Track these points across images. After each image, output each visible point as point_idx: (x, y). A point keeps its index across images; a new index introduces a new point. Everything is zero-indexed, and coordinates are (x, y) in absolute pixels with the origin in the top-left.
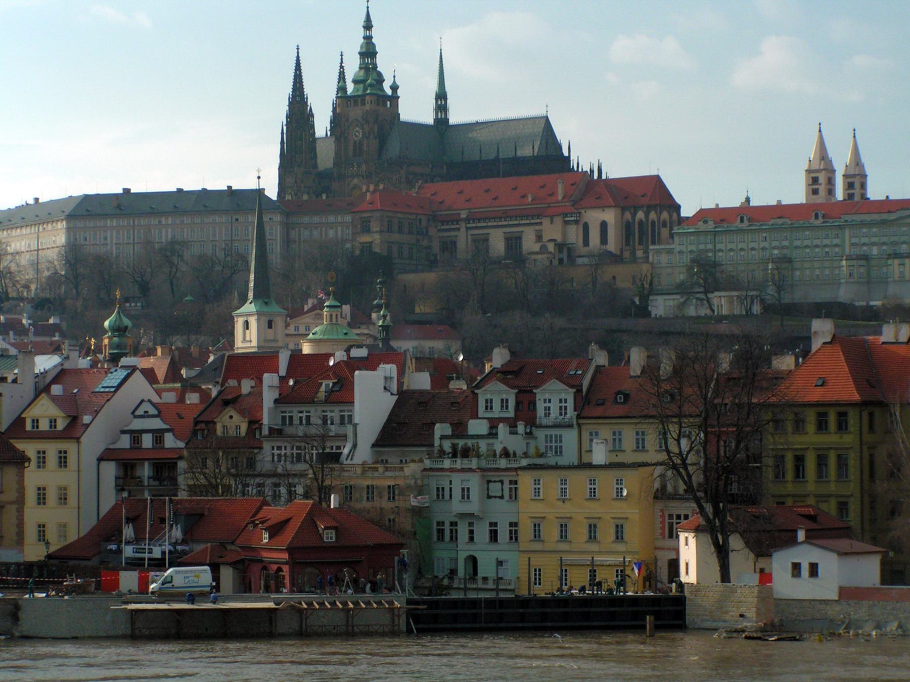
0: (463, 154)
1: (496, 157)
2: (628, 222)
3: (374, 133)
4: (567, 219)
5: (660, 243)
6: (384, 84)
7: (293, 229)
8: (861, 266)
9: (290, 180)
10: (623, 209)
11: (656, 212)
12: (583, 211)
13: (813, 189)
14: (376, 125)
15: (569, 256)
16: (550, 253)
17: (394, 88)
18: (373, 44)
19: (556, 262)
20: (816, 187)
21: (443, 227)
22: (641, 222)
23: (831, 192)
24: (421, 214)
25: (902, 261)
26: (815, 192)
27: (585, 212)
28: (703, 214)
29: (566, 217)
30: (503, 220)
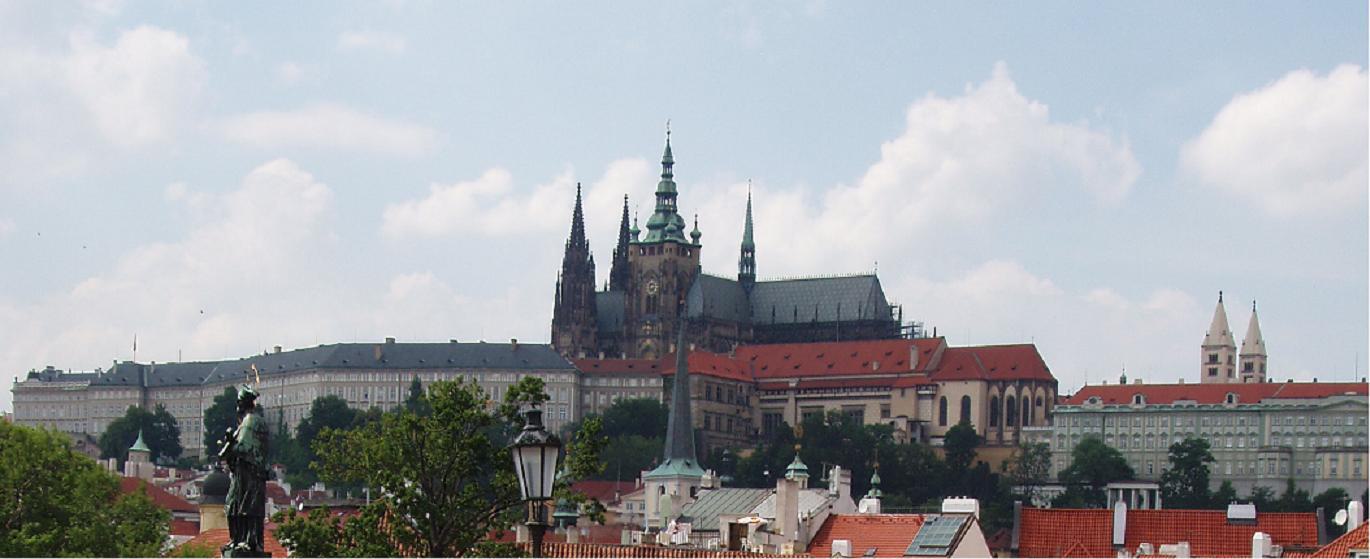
0: (774, 315)
1: (813, 320)
2: (995, 398)
3: (673, 287)
4: (920, 392)
5: (1033, 423)
6: (684, 230)
7: (588, 393)
8: (1283, 459)
9: (566, 340)
10: (989, 383)
11: (1031, 389)
12: (940, 384)
13: (1210, 369)
14: (675, 279)
15: (922, 436)
16: (900, 430)
17: (696, 236)
18: (674, 184)
19: (907, 441)
20: (1215, 366)
21: (766, 397)
22: (1011, 399)
23: (1230, 373)
24: (744, 381)
25: (1333, 456)
26: (1213, 372)
27: (944, 384)
28: (1087, 392)
29: (920, 389)
30: (842, 390)
